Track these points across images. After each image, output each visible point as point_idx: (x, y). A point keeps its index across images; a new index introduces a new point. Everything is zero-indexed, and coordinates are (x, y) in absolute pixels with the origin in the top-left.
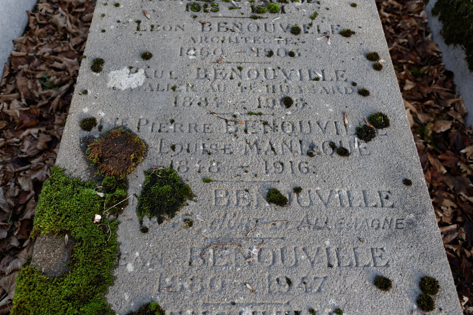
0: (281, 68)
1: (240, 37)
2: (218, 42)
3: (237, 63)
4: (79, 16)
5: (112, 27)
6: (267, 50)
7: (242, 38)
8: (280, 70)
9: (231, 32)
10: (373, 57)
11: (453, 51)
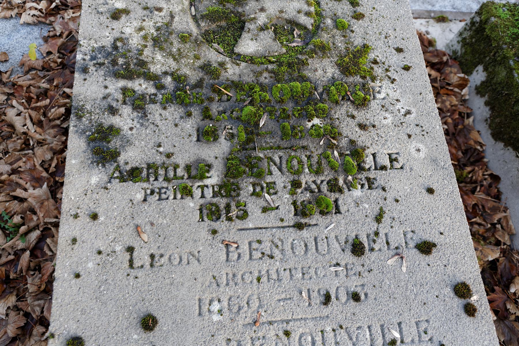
0: (344, 327)
1: (283, 269)
2: (251, 282)
3: (282, 321)
4: (42, 111)
5: (90, 265)
6: (322, 293)
7: (285, 270)
8: (342, 331)
9: (269, 261)
10: (462, 290)
11: (502, 152)
